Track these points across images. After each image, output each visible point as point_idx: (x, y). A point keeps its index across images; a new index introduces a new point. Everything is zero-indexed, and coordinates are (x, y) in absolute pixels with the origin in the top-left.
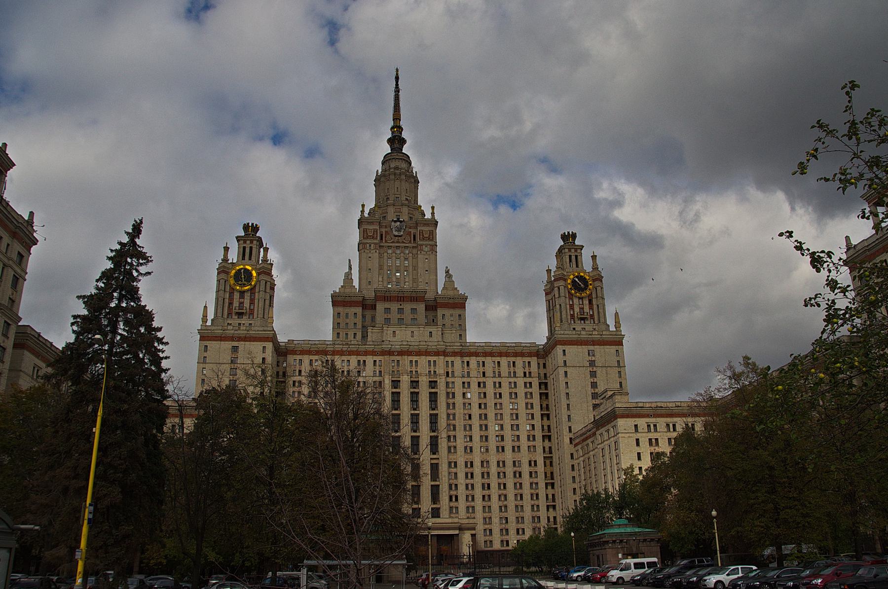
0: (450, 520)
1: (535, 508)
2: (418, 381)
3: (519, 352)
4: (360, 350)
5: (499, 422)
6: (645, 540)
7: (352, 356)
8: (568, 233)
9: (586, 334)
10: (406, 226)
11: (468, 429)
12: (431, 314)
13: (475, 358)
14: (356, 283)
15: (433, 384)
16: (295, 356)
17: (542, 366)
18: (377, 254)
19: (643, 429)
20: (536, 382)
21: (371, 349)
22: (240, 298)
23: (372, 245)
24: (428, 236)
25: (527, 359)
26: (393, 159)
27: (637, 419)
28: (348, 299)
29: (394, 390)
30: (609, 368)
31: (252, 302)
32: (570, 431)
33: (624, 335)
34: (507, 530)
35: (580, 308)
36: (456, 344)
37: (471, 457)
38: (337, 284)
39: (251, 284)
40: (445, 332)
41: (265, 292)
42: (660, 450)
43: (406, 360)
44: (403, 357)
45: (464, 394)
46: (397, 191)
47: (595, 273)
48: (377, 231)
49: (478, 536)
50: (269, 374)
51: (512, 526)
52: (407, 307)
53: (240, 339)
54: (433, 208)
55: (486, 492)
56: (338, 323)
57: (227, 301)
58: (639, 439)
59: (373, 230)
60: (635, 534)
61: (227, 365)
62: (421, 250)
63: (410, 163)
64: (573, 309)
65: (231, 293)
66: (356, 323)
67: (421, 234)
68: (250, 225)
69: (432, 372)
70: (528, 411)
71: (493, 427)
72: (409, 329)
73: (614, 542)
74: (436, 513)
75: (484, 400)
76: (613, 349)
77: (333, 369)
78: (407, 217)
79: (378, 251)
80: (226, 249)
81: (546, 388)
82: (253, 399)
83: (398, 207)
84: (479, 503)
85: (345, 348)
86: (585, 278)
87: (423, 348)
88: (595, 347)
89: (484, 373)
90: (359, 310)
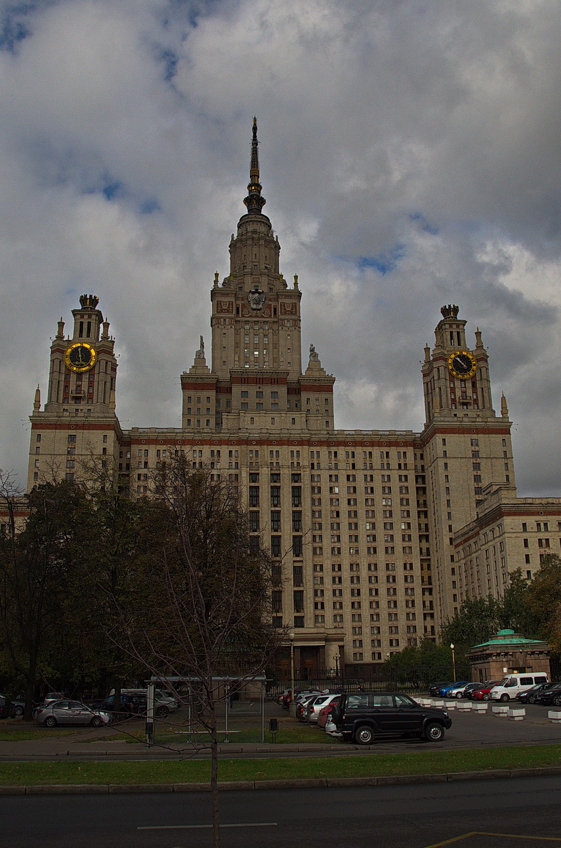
0: (314, 631)
1: (411, 616)
2: (279, 474)
3: (393, 442)
4: (213, 438)
5: (370, 520)
6: (533, 653)
7: (205, 446)
8: (450, 306)
9: (469, 421)
10: (265, 298)
11: (335, 527)
12: (294, 398)
13: (343, 447)
14: (209, 363)
15: (296, 477)
16: (140, 446)
17: (418, 456)
18: (233, 330)
19: (532, 528)
20: (412, 476)
21: (227, 438)
22: (77, 381)
23: (227, 320)
24: (290, 309)
25: (402, 449)
26: (250, 221)
27: (525, 517)
28: (199, 381)
29: (253, 484)
30: (494, 460)
31: (91, 384)
32: (450, 530)
33: (512, 423)
34: (379, 641)
35: (462, 392)
36: (323, 432)
37: (339, 559)
39: (89, 365)
40: (310, 418)
41: (106, 373)
42: (552, 552)
43: (265, 450)
44: (262, 446)
45: (331, 488)
46: (256, 258)
47: (479, 352)
48: (233, 304)
49: (346, 649)
50: (110, 466)
51: (385, 637)
52: (267, 390)
53: (78, 427)
54: (296, 277)
55: (356, 599)
56: (189, 409)
57: (62, 384)
58: (527, 539)
59: (228, 303)
60: (522, 645)
61: (63, 456)
62: (283, 325)
63: (270, 227)
64: (455, 393)
65: (67, 375)
66: (209, 409)
67: (283, 307)
68: (88, 297)
69: (295, 464)
70: (403, 508)
71: (364, 526)
72: (269, 415)
73: (498, 654)
74: (299, 622)
75: (354, 495)
76: (499, 437)
77: (183, 461)
78: (267, 288)
79: (233, 327)
80: (61, 325)
81: (424, 483)
82: (93, 496)
83: (257, 277)
84: (347, 611)
85: (197, 437)
86: (468, 358)
87: (285, 436)
88: (479, 435)
89: (353, 465)
90: (212, 394)
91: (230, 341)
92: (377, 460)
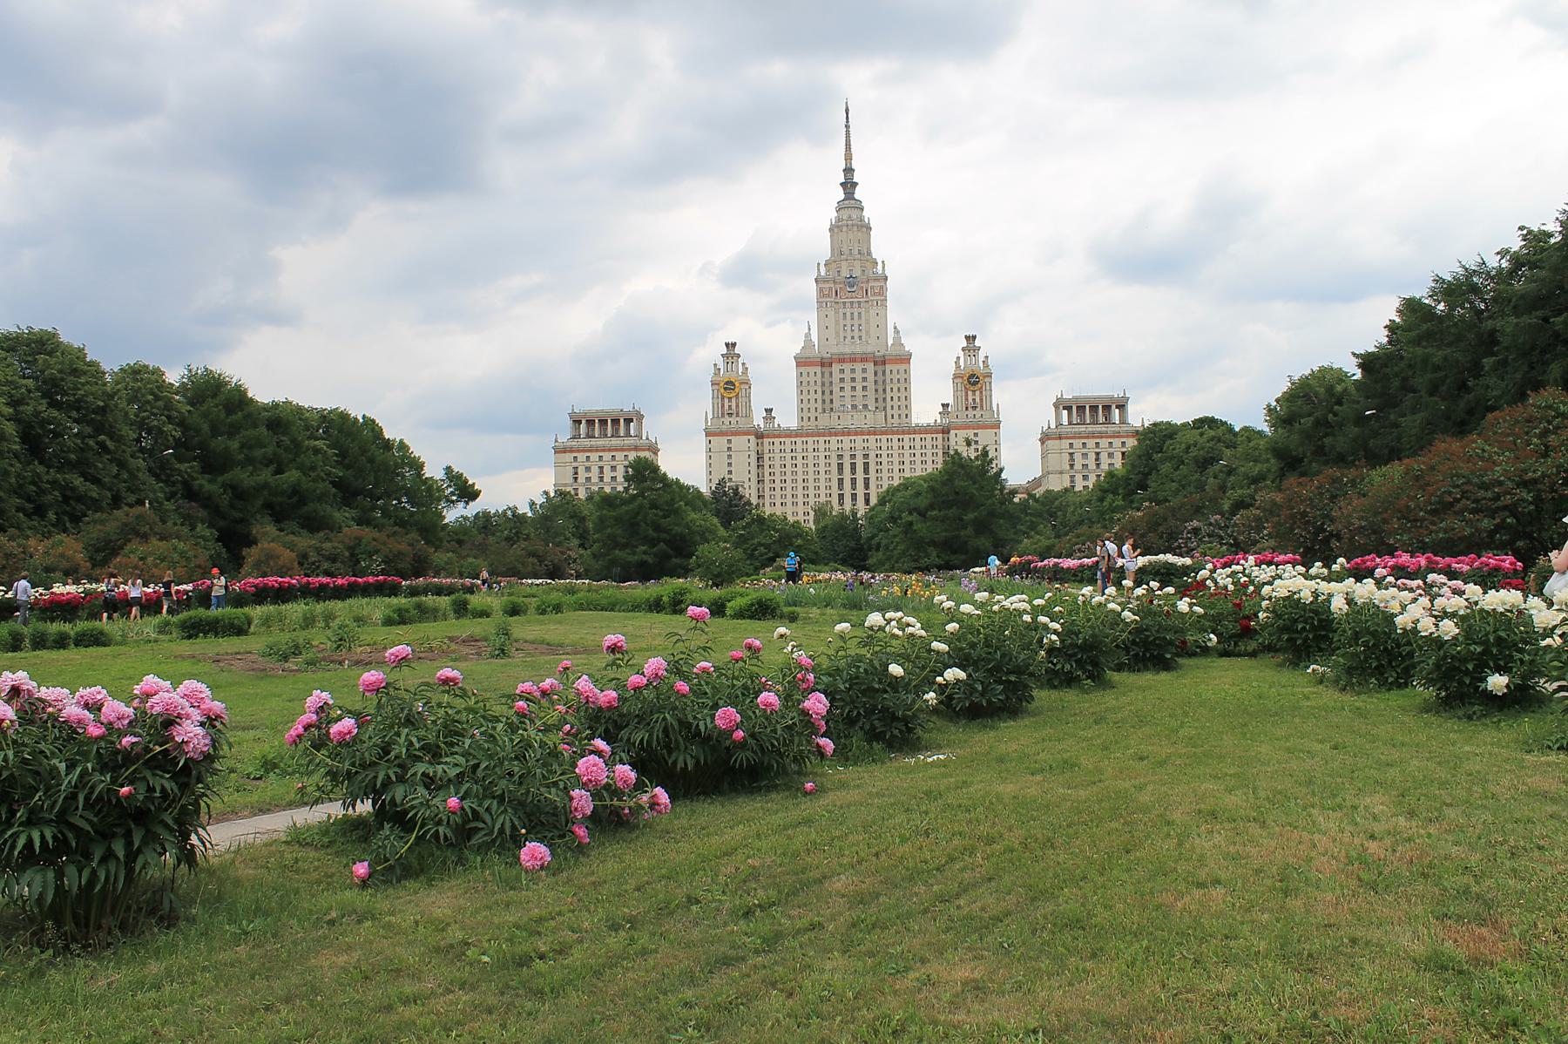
15: (866, 456)
38: (797, 348)
52: (859, 367)
91: (831, 322)
92: (918, 443)
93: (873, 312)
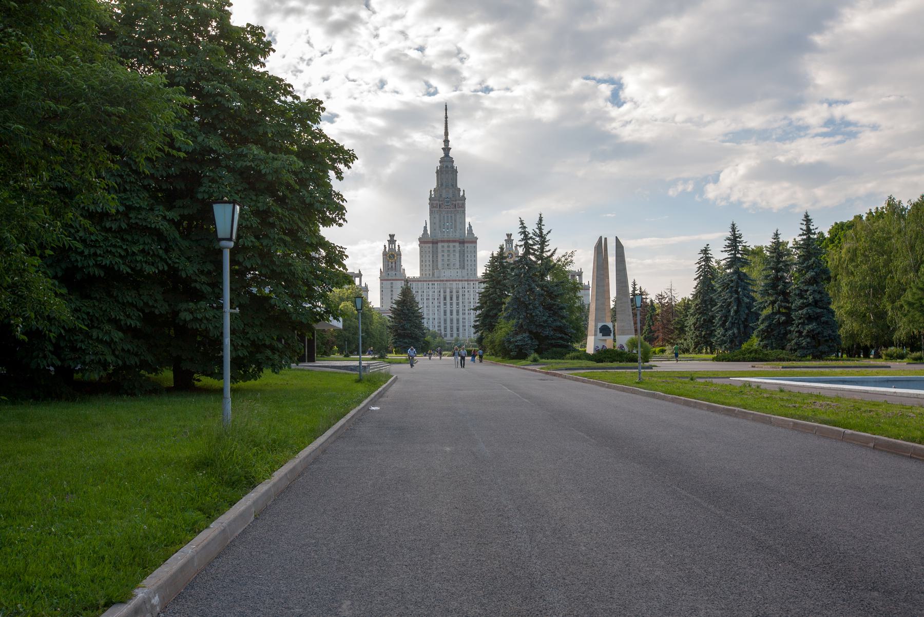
14: (429, 232)
15: (457, 292)
52: (451, 245)
53: (393, 280)
63: (453, 162)
90: (431, 245)
91: (437, 221)
93: (458, 216)
